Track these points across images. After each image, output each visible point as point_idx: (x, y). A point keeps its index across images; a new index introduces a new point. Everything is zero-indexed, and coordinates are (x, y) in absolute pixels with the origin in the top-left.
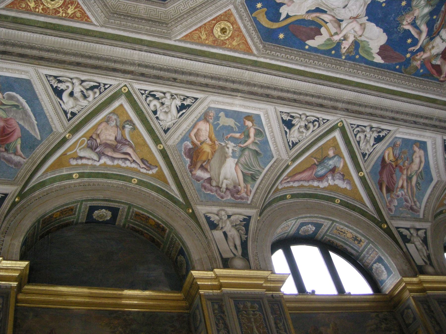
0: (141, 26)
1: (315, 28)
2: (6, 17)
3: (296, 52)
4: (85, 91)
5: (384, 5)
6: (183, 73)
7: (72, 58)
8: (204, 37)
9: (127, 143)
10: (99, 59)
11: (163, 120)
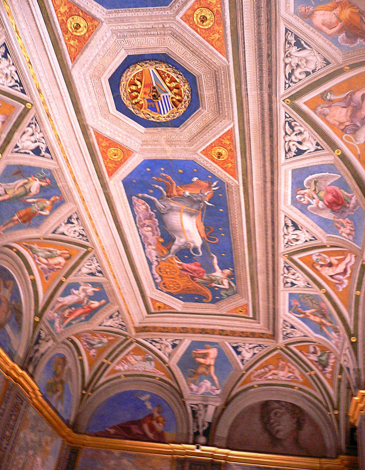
0: (224, 92)
2: (244, 180)
4: (295, 133)
6: (260, 48)
7: (266, 141)
8: (217, 36)
9: (349, 97)
10: (263, 122)
11: (316, 65)
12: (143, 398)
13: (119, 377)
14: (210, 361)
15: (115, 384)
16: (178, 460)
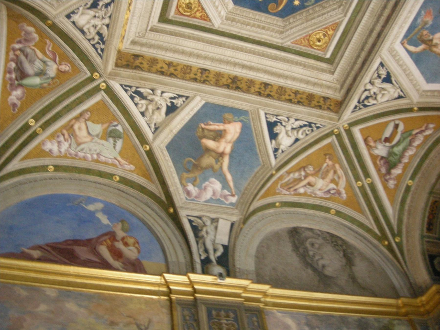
12: (91, 208)
13: (44, 168)
14: (225, 146)
15: (35, 181)
16: (180, 302)
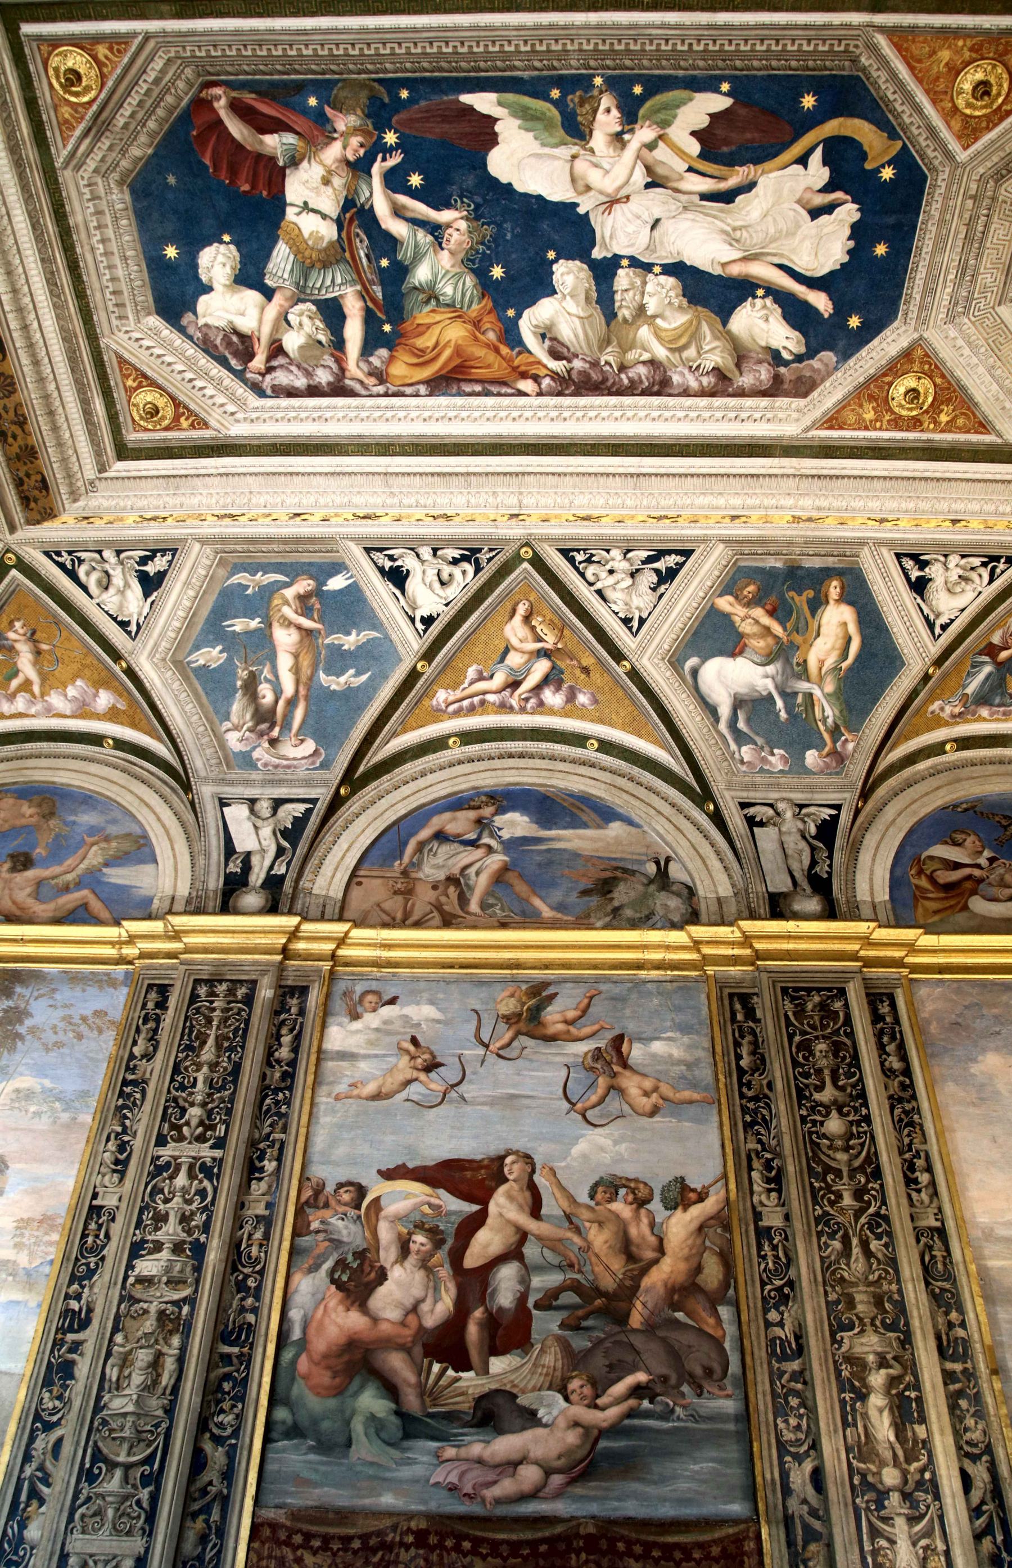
1: (717, 145)
3: (756, 63)
5: (551, 255)
